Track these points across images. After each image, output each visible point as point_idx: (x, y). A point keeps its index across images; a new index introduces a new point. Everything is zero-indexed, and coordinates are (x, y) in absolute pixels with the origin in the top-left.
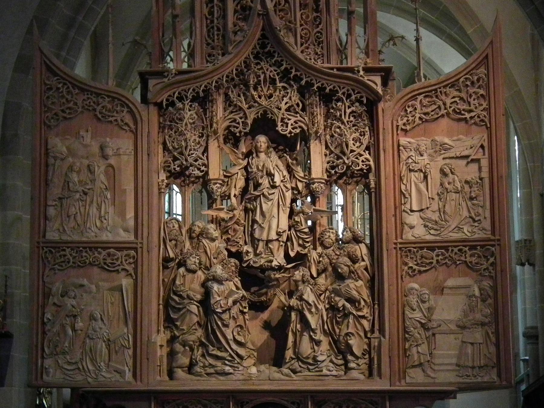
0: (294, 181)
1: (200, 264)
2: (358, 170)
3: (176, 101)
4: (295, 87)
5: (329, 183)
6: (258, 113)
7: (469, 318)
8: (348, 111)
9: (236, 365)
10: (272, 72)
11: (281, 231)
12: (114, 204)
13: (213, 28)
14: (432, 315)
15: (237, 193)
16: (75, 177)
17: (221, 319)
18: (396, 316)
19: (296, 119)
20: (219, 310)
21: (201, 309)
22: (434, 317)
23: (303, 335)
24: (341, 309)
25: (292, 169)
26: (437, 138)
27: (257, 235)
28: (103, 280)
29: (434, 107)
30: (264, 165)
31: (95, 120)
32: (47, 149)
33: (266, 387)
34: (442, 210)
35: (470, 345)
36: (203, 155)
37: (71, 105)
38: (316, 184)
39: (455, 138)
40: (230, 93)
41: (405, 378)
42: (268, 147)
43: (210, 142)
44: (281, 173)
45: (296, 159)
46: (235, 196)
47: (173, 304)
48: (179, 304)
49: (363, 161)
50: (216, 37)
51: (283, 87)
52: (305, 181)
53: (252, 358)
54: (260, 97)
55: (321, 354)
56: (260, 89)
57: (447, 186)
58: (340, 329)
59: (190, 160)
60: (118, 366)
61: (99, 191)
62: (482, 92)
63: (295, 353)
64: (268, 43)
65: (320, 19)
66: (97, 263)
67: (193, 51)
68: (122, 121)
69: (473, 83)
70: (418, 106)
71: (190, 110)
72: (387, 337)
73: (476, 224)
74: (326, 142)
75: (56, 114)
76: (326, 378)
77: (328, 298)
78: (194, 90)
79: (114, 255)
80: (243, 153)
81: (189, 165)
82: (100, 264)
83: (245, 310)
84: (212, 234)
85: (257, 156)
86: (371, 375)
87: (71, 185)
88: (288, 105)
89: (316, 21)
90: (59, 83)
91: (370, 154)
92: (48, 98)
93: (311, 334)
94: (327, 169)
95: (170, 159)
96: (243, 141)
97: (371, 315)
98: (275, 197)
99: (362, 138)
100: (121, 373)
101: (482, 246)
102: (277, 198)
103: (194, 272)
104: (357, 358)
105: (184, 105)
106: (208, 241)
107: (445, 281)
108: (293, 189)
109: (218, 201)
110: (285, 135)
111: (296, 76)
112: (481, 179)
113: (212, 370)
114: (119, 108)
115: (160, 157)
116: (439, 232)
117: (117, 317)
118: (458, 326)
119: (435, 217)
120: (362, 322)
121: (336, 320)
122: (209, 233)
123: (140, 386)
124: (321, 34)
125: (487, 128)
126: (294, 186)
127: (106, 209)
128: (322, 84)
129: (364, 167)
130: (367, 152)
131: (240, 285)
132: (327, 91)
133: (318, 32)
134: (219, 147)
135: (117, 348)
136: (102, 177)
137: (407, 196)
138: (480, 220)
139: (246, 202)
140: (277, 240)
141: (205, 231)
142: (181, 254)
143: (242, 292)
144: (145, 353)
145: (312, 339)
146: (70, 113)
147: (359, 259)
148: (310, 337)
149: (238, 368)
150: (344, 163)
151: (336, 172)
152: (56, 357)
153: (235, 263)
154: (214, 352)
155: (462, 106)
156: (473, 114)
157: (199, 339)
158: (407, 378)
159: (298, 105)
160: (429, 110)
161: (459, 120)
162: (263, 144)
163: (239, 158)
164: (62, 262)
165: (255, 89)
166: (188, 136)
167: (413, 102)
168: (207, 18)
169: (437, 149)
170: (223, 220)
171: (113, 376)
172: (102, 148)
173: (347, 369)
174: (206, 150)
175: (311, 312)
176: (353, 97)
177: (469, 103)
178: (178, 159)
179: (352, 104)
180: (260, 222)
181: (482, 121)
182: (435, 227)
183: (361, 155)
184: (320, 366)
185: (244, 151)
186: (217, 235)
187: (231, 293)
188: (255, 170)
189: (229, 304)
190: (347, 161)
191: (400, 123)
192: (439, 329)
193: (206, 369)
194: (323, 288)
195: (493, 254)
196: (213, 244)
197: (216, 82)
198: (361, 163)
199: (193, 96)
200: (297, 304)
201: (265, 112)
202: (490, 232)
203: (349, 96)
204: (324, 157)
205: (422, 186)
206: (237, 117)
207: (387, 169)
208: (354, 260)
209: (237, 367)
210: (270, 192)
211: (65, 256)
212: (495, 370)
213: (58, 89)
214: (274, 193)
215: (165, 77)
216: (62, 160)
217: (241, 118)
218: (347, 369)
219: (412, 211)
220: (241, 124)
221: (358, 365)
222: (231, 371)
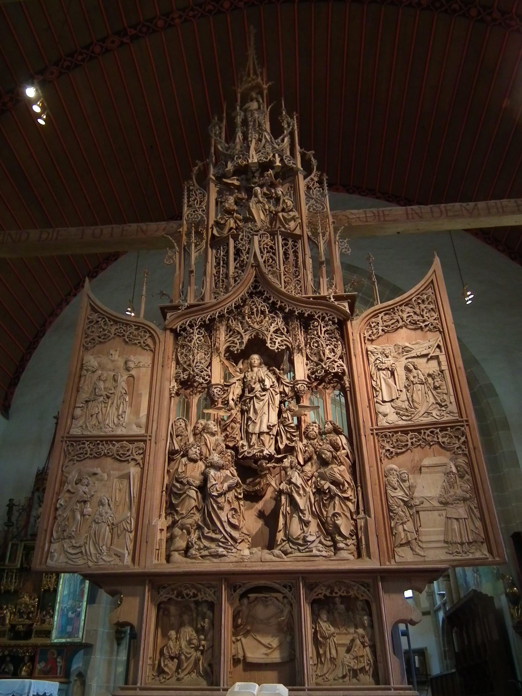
1: (201, 454)
3: (188, 328)
6: (251, 335)
9: (229, 547)
12: (131, 405)
13: (219, 281)
15: (235, 398)
16: (102, 385)
17: (217, 502)
19: (282, 339)
20: (215, 494)
21: (199, 494)
23: (293, 517)
28: (114, 470)
31: (123, 344)
32: (82, 364)
37: (106, 332)
38: (300, 385)
42: (260, 364)
43: (213, 358)
44: (270, 380)
45: (283, 369)
46: (233, 400)
47: (175, 490)
49: (338, 366)
53: (246, 542)
55: (310, 535)
58: (327, 512)
59: (196, 371)
61: (119, 394)
63: (285, 535)
64: (259, 286)
65: (299, 272)
67: (204, 296)
68: (144, 343)
71: (198, 334)
74: (307, 355)
75: (93, 339)
77: (315, 483)
78: (202, 319)
79: (125, 447)
80: (240, 369)
81: (195, 375)
82: (113, 455)
83: (240, 496)
84: (212, 429)
86: (360, 556)
87: (97, 390)
88: (275, 328)
89: (296, 273)
90: (100, 318)
91: (343, 361)
92: (89, 328)
93: (300, 514)
95: (180, 371)
97: (355, 498)
99: (335, 349)
100: (120, 556)
102: (267, 398)
103: (195, 461)
104: (345, 538)
105: (193, 329)
106: (209, 436)
108: (281, 393)
110: (274, 350)
113: (206, 553)
114: (142, 334)
115: (172, 370)
117: (123, 502)
121: (323, 503)
122: (209, 428)
123: (137, 569)
124: (300, 282)
127: (123, 408)
128: (302, 311)
129: (339, 370)
130: (341, 360)
131: (235, 473)
132: (306, 315)
133: (298, 280)
134: (221, 361)
135: (119, 532)
136: (124, 385)
139: (242, 405)
141: (207, 426)
144: (144, 537)
145: (301, 520)
146: (103, 339)
147: (340, 447)
148: (300, 518)
149: (232, 550)
150: (323, 368)
151: (316, 376)
153: (231, 453)
154: (209, 535)
159: (283, 329)
162: (256, 360)
168: (215, 276)
171: (113, 559)
172: (126, 363)
173: (337, 550)
174: (210, 364)
175: (299, 495)
176: (327, 319)
178: (188, 370)
179: (327, 325)
180: (253, 419)
183: (336, 362)
184: (310, 546)
186: (216, 430)
187: (226, 478)
189: (224, 488)
190: (324, 366)
193: (201, 551)
194: (310, 474)
196: (213, 439)
198: (336, 368)
200: (287, 487)
201: (257, 333)
203: (323, 319)
204: (305, 366)
206: (236, 340)
207: (359, 369)
208: (336, 448)
209: (230, 549)
213: (98, 322)
214: (265, 395)
215: (180, 310)
216: (94, 372)
217: (238, 340)
220: (238, 344)
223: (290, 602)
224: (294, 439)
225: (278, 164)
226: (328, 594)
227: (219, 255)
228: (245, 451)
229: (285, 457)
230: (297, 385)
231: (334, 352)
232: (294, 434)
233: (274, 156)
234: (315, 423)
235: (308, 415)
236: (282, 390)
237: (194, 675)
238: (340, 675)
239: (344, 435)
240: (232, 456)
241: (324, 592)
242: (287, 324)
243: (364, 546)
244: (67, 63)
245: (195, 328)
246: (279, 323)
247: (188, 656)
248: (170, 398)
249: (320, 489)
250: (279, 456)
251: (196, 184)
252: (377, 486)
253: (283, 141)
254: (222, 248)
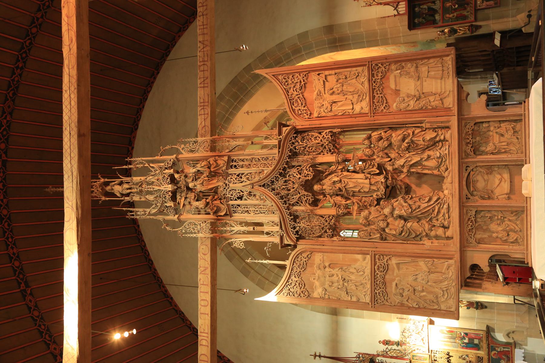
1: (383, 220)
2: (332, 138)
3: (296, 230)
4: (289, 170)
5: (339, 153)
7: (413, 74)
8: (301, 143)
9: (443, 202)
10: (281, 182)
14: (412, 95)
18: (412, 115)
20: (410, 210)
22: (413, 94)
25: (331, 172)
26: (314, 98)
27: (367, 190)
29: (298, 100)
30: (329, 186)
33: (457, 185)
34: (353, 93)
35: (429, 73)
36: (323, 217)
38: (339, 159)
39: (314, 89)
40: (292, 203)
41: (450, 108)
42: (320, 184)
47: (406, 235)
48: (407, 232)
49: (327, 135)
50: (264, 209)
51: (289, 176)
54: (294, 188)
56: (289, 188)
57: (339, 91)
60: (445, 267)
62: (291, 77)
63: (434, 169)
66: (383, 276)
69: (286, 82)
70: (298, 108)
72: (425, 119)
73: (360, 75)
74: (316, 154)
76: (450, 151)
78: (290, 221)
85: (324, 190)
86: (448, 128)
88: (298, 174)
91: (323, 132)
94: (331, 154)
96: (317, 197)
98: (346, 180)
101: (372, 71)
102: (346, 180)
103: (388, 224)
104: (438, 135)
107: (392, 89)
108: (342, 171)
109: (349, 210)
110: (313, 175)
111: (283, 170)
112: (336, 74)
113: (447, 216)
116: (364, 94)
118: (418, 80)
119: (356, 96)
123: (457, 256)
125: (309, 73)
126: (340, 171)
128: (287, 156)
129: (330, 135)
131: (395, 200)
132: (290, 154)
137: (345, 112)
138: (358, 73)
140: (370, 179)
142: (378, 230)
143: (400, 198)
150: (327, 145)
152: (439, 302)
154: (436, 214)
155: (298, 86)
156: (302, 80)
157: (427, 222)
158: (450, 106)
159: (298, 169)
160: (300, 102)
161: (305, 87)
163: (326, 199)
164: (383, 295)
165: (289, 190)
166: (314, 225)
167: (296, 111)
169: (320, 97)
170: (358, 208)
175: (411, 160)
176: (293, 141)
177: (296, 83)
181: (305, 76)
182: (362, 96)
183: (324, 136)
185: (322, 196)
188: (332, 191)
190: (327, 143)
191: (307, 117)
192: (420, 91)
194: (397, 155)
195: (377, 65)
196: (372, 213)
197: (286, 209)
198: (328, 136)
199: (293, 221)
201: (301, 185)
202: (365, 67)
203: (293, 143)
205: (340, 104)
206: (304, 200)
207: (331, 122)
208: (381, 138)
209: (445, 201)
210: (343, 182)
211: (379, 293)
212: (444, 58)
215: (283, 235)
217: (305, 198)
218: (445, 140)
219: (353, 108)
221: (442, 134)
222: (447, 204)
223: (475, 167)
225: (172, 171)
226: (471, 146)
227: (240, 211)
229: (386, 170)
231: (316, 137)
233: (165, 174)
234: (363, 150)
237: (518, 223)
238: (517, 140)
240: (385, 201)
241: (470, 148)
242: (293, 166)
243: (442, 124)
244: (47, 337)
245: (296, 225)
246: (293, 171)
247: (507, 225)
248: (344, 241)
251: (181, 228)
252: (407, 115)
253: (153, 167)
254: (235, 209)
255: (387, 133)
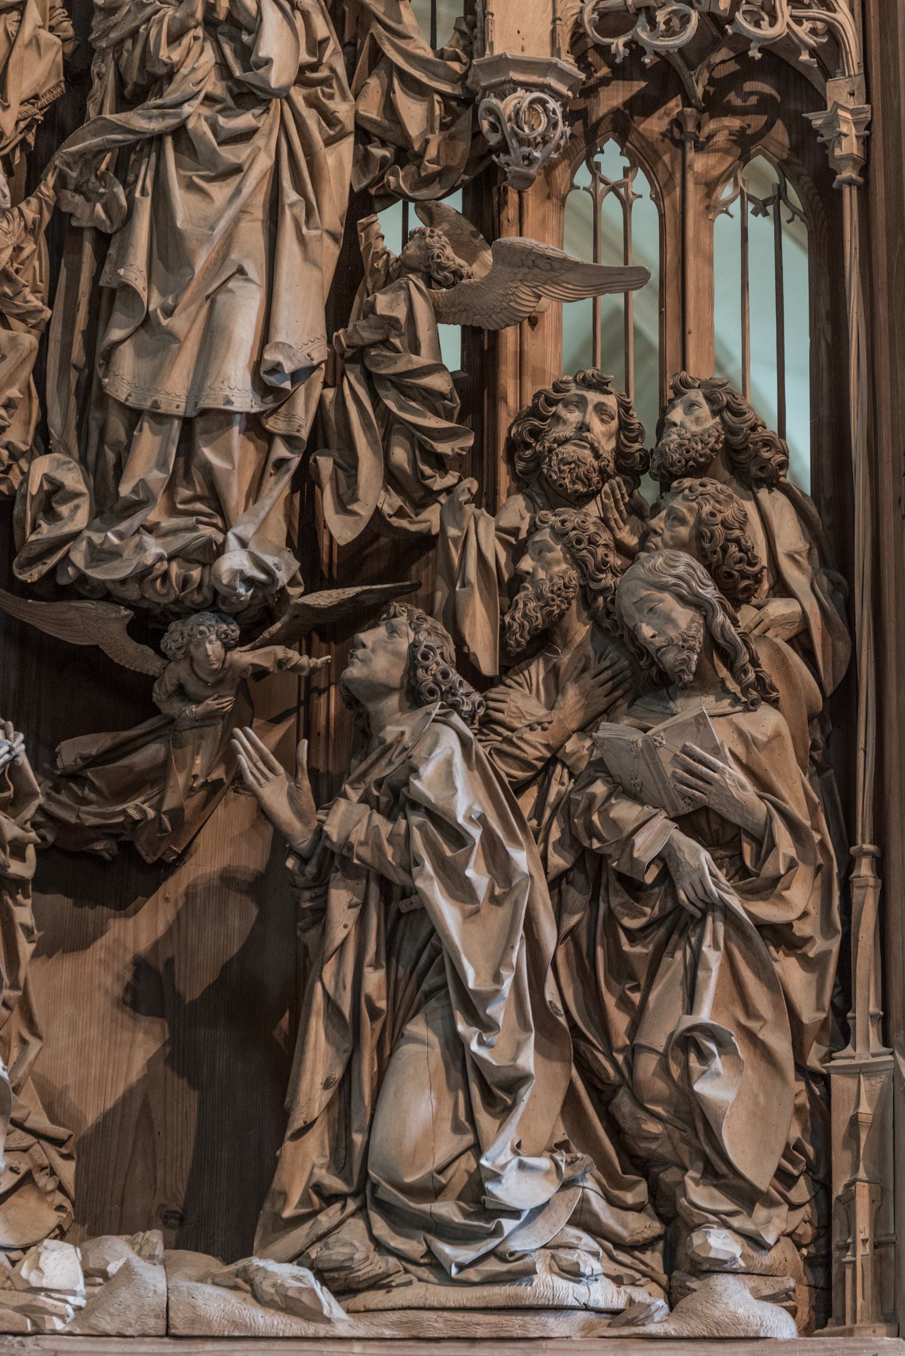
0: (374, 84)
11: (288, 367)
24: (649, 878)
38: (522, 98)
44: (299, 23)
52: (446, 88)
55: (522, 1166)
77: (565, 807)
102: (264, 162)
120: (777, 967)
126: (371, 108)
180: (155, 302)
224: (439, 483)
228: (75, 536)
230: (502, 90)
232: (443, 448)
235: (548, 324)
236: (371, 108)
239: (787, 491)
249: (601, 859)
250: (323, 599)
255: (795, 659)
